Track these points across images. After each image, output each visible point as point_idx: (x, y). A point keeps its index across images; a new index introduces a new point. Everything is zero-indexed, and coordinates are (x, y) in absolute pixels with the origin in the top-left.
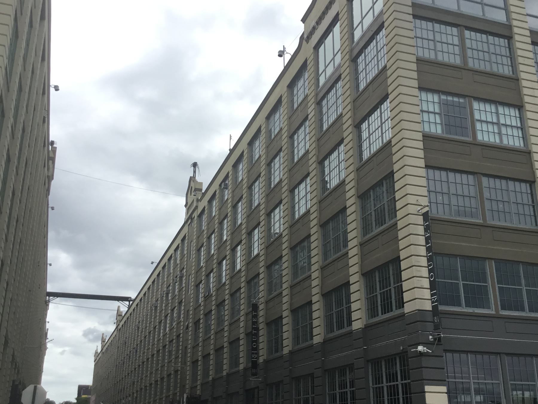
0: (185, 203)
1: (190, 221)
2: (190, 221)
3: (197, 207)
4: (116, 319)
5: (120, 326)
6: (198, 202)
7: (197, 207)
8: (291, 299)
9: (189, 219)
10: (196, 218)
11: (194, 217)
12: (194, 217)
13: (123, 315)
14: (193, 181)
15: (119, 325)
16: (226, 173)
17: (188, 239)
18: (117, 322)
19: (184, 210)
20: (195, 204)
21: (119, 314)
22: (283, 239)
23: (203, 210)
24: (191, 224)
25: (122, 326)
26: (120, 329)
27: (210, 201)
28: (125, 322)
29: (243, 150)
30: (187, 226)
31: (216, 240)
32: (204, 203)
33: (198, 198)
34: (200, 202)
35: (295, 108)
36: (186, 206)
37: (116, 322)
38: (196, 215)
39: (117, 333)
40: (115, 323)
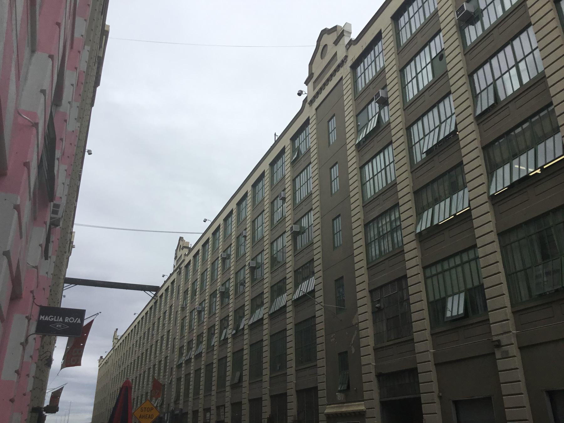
2: (178, 270)
3: (183, 261)
4: (113, 341)
5: (116, 347)
7: (183, 261)
9: (177, 269)
10: (183, 268)
13: (119, 338)
14: (182, 241)
15: (115, 346)
23: (189, 263)
25: (118, 347)
26: (116, 349)
27: (195, 256)
30: (175, 274)
32: (191, 257)
36: (175, 259)
38: (183, 266)
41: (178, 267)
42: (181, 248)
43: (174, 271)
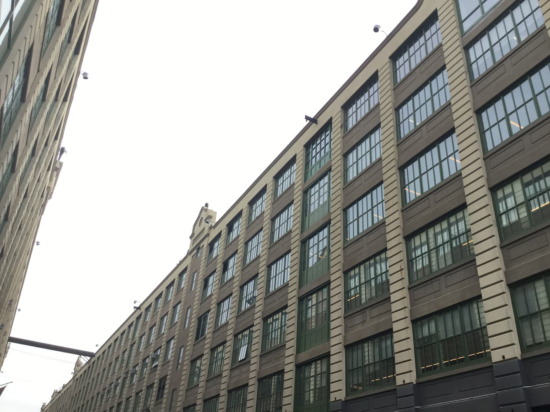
0: (190, 233)
1: (195, 251)
2: (195, 251)
3: (208, 235)
4: (74, 369)
5: (78, 375)
6: (210, 229)
7: (208, 235)
8: (260, 368)
9: (196, 249)
10: (206, 245)
11: (203, 246)
12: (203, 246)
15: (76, 375)
16: (239, 211)
17: (190, 271)
18: (75, 372)
19: (189, 241)
20: (206, 232)
21: (78, 364)
22: (256, 309)
23: (219, 235)
24: (196, 255)
25: (81, 376)
26: (77, 379)
28: (85, 372)
29: (221, 231)
30: (190, 257)
31: (181, 308)
33: (212, 225)
34: (214, 229)
35: (278, 195)
36: (191, 237)
37: (73, 371)
38: (206, 243)
39: (73, 383)
40: (72, 373)
41: (195, 247)
42: (204, 219)
43: (189, 253)
